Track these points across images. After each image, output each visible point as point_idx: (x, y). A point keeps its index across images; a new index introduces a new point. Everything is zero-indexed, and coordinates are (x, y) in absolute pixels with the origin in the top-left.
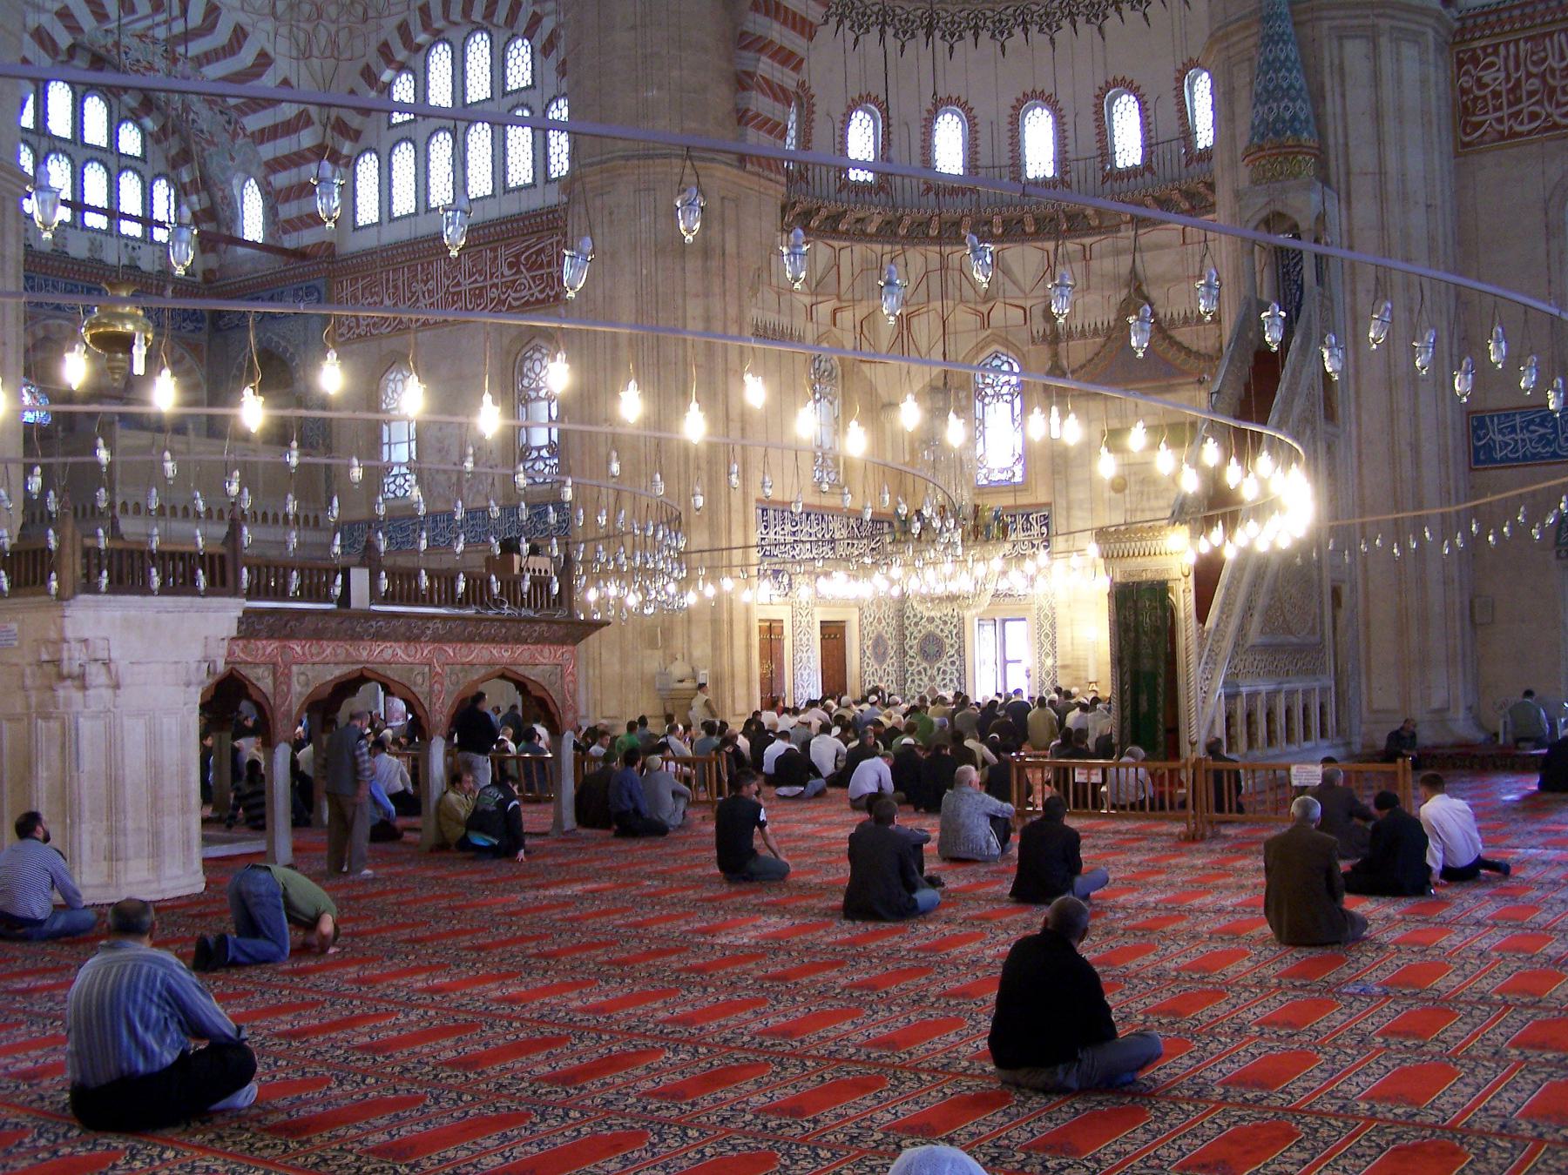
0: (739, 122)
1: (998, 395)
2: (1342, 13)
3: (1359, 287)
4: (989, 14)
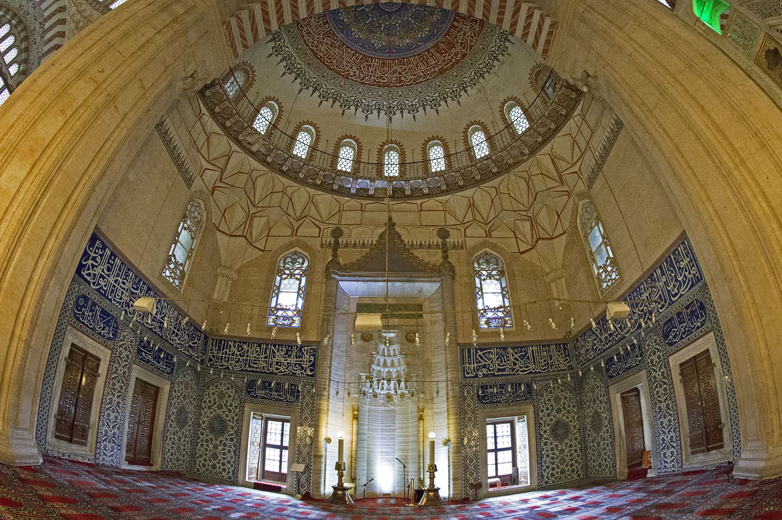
1: (292, 275)
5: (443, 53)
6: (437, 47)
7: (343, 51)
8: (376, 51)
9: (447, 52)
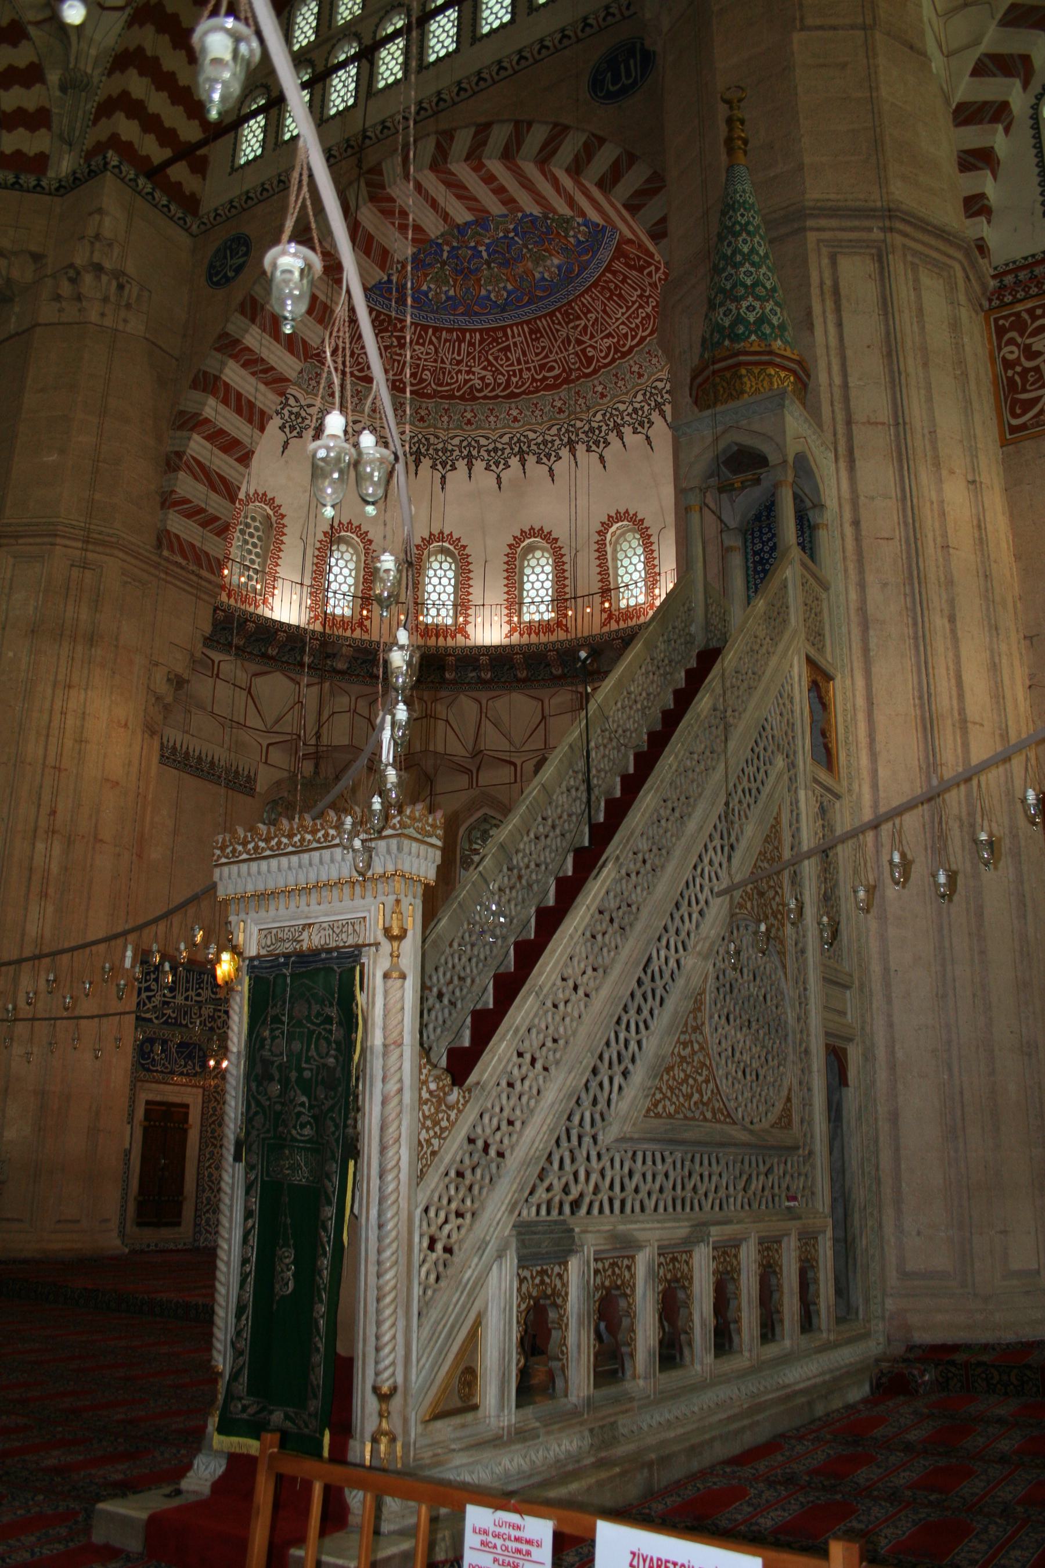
0: (163, 505)
2: (834, 223)
3: (870, 578)
4: (483, 441)
5: (645, 268)
6: (626, 257)
7: (431, 342)
8: (503, 310)
9: (650, 264)
